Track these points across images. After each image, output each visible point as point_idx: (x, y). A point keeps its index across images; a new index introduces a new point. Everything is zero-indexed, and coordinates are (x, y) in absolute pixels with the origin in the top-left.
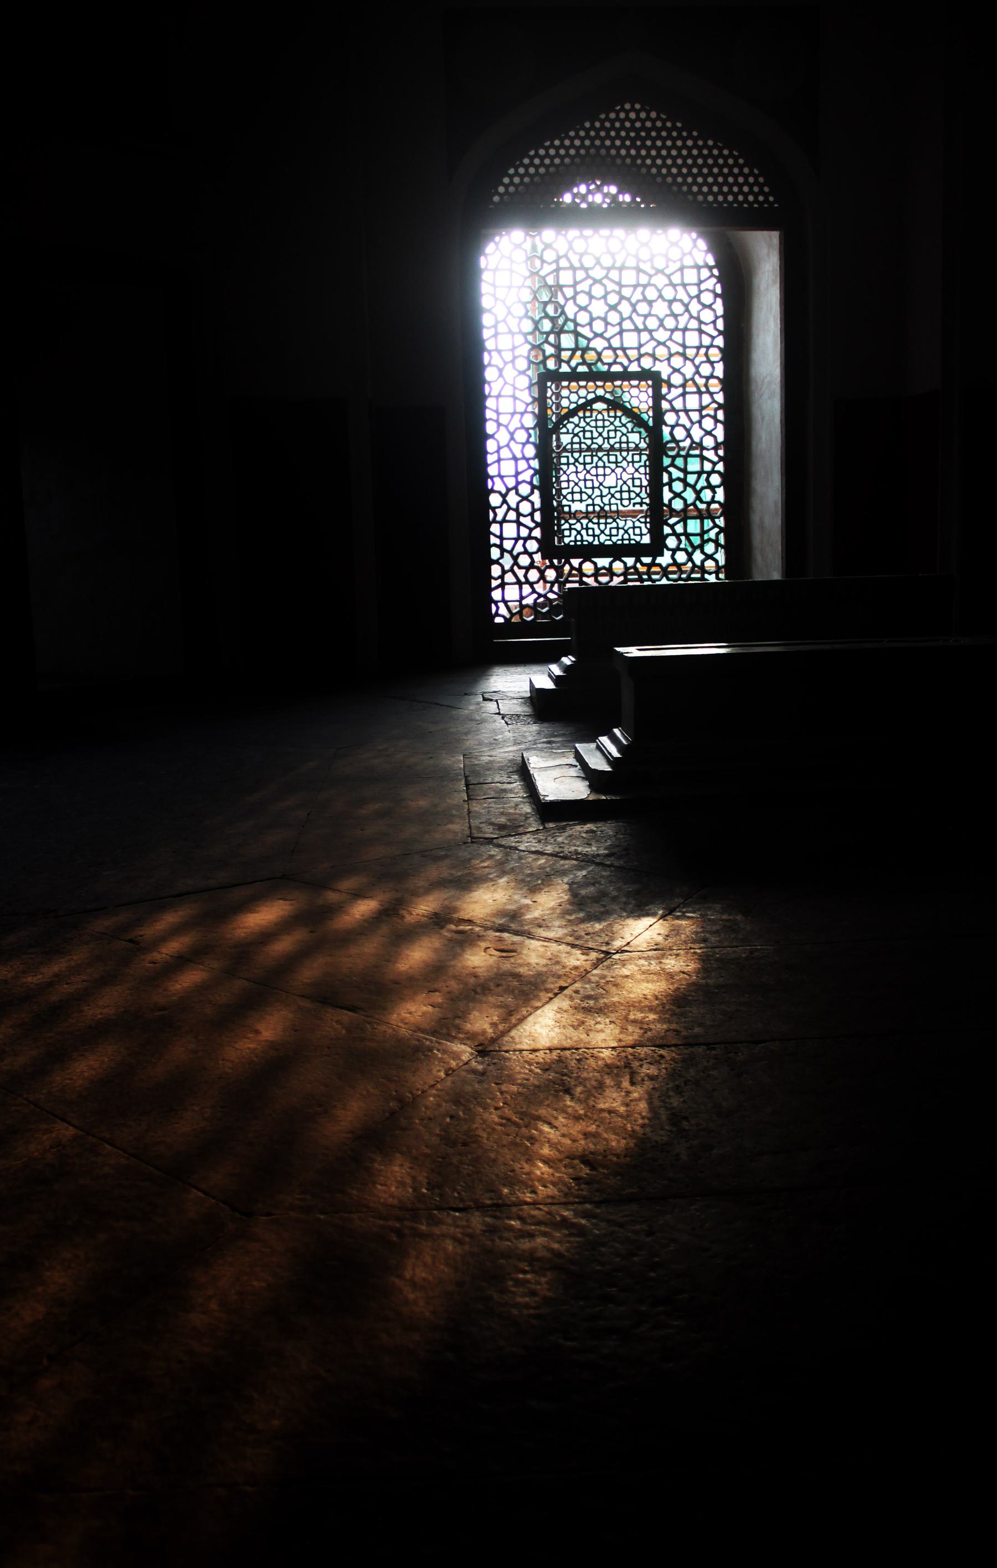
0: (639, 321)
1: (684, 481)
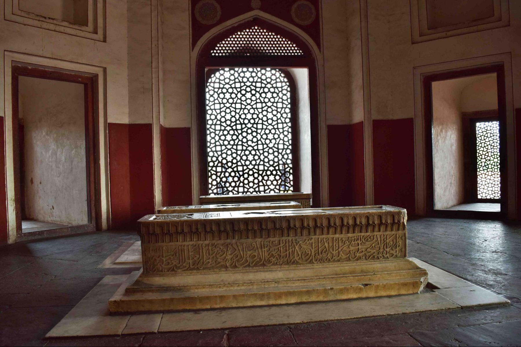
0: (262, 100)
1: (278, 152)
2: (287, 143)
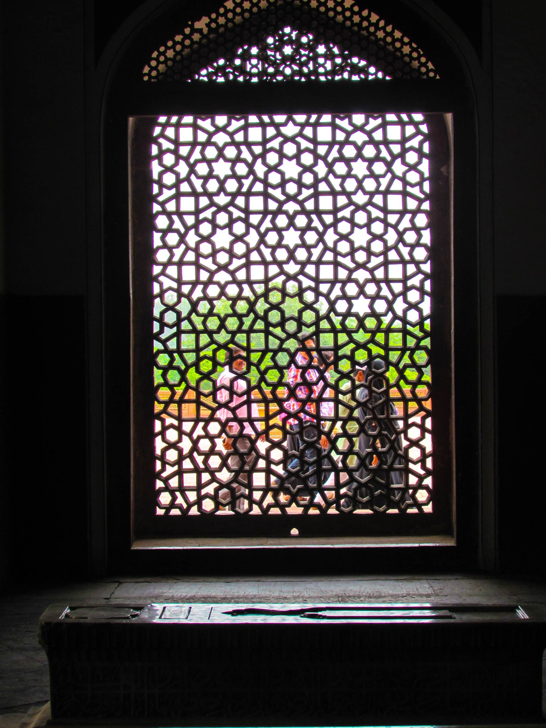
0: (336, 183)
2: (416, 331)
